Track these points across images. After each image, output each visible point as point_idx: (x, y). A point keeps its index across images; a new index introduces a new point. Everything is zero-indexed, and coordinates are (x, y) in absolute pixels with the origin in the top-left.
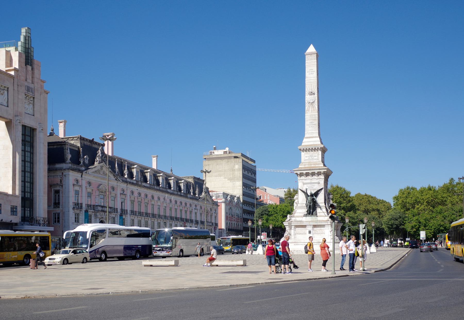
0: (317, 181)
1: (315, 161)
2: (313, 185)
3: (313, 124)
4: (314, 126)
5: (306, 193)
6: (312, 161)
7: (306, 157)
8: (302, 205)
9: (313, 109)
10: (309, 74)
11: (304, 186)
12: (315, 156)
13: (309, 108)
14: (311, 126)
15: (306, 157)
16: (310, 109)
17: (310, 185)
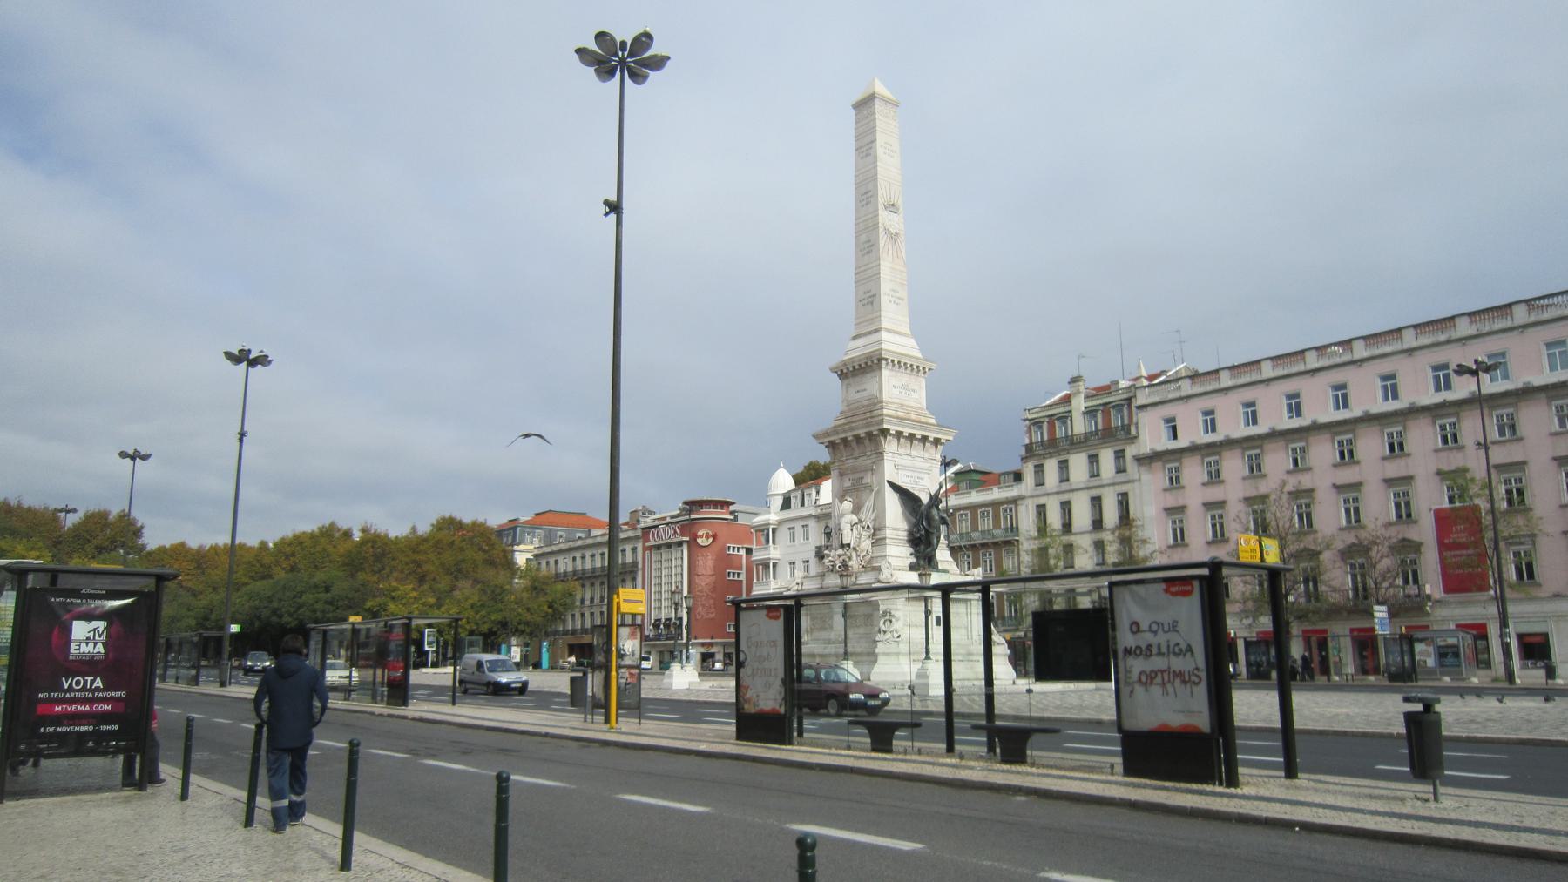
0: (927, 465)
1: (913, 404)
2: (919, 475)
3: (898, 295)
4: (897, 301)
5: (908, 498)
6: (906, 403)
7: (894, 387)
8: (895, 532)
9: (895, 254)
10: (885, 153)
11: (898, 473)
12: (914, 391)
13: (887, 247)
14: (893, 299)
15: (894, 387)
16: (890, 252)
17: (909, 474)
